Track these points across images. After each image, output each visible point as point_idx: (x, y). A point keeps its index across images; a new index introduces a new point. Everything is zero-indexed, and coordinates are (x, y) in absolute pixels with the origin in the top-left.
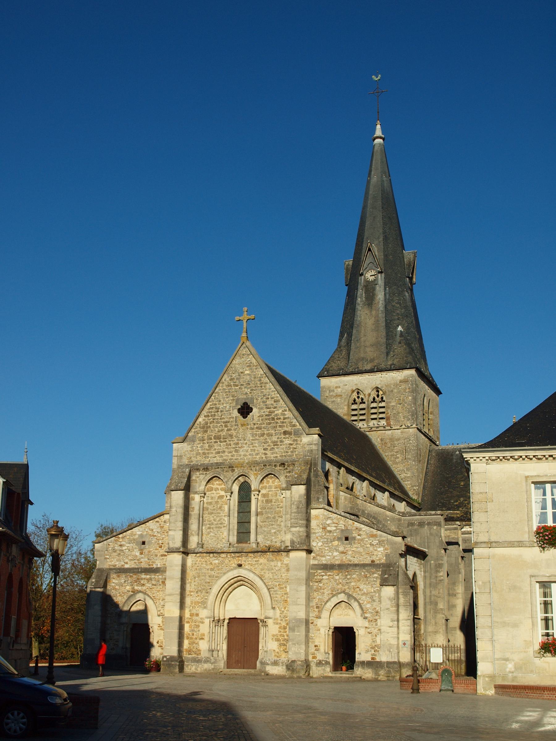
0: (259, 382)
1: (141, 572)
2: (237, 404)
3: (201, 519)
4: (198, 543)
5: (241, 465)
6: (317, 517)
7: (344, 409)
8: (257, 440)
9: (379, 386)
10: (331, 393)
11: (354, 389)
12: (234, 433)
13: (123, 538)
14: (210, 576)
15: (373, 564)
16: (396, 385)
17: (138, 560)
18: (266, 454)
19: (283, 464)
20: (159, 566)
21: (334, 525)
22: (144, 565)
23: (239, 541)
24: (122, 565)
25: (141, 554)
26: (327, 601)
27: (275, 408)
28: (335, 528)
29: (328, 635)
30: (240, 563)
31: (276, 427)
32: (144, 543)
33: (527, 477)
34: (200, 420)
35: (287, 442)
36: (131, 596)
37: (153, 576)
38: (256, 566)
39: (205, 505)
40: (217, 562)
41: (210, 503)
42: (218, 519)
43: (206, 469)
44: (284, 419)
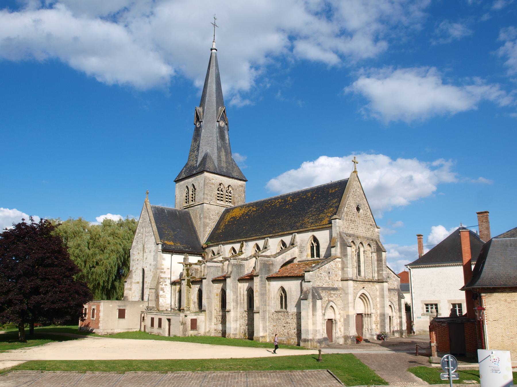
7: (215, 192)
9: (231, 185)
10: (210, 182)
13: (321, 269)
16: (238, 187)
17: (328, 283)
18: (366, 233)
19: (372, 240)
20: (336, 287)
22: (331, 286)
24: (322, 285)
25: (329, 279)
32: (329, 272)
37: (336, 292)
40: (356, 285)
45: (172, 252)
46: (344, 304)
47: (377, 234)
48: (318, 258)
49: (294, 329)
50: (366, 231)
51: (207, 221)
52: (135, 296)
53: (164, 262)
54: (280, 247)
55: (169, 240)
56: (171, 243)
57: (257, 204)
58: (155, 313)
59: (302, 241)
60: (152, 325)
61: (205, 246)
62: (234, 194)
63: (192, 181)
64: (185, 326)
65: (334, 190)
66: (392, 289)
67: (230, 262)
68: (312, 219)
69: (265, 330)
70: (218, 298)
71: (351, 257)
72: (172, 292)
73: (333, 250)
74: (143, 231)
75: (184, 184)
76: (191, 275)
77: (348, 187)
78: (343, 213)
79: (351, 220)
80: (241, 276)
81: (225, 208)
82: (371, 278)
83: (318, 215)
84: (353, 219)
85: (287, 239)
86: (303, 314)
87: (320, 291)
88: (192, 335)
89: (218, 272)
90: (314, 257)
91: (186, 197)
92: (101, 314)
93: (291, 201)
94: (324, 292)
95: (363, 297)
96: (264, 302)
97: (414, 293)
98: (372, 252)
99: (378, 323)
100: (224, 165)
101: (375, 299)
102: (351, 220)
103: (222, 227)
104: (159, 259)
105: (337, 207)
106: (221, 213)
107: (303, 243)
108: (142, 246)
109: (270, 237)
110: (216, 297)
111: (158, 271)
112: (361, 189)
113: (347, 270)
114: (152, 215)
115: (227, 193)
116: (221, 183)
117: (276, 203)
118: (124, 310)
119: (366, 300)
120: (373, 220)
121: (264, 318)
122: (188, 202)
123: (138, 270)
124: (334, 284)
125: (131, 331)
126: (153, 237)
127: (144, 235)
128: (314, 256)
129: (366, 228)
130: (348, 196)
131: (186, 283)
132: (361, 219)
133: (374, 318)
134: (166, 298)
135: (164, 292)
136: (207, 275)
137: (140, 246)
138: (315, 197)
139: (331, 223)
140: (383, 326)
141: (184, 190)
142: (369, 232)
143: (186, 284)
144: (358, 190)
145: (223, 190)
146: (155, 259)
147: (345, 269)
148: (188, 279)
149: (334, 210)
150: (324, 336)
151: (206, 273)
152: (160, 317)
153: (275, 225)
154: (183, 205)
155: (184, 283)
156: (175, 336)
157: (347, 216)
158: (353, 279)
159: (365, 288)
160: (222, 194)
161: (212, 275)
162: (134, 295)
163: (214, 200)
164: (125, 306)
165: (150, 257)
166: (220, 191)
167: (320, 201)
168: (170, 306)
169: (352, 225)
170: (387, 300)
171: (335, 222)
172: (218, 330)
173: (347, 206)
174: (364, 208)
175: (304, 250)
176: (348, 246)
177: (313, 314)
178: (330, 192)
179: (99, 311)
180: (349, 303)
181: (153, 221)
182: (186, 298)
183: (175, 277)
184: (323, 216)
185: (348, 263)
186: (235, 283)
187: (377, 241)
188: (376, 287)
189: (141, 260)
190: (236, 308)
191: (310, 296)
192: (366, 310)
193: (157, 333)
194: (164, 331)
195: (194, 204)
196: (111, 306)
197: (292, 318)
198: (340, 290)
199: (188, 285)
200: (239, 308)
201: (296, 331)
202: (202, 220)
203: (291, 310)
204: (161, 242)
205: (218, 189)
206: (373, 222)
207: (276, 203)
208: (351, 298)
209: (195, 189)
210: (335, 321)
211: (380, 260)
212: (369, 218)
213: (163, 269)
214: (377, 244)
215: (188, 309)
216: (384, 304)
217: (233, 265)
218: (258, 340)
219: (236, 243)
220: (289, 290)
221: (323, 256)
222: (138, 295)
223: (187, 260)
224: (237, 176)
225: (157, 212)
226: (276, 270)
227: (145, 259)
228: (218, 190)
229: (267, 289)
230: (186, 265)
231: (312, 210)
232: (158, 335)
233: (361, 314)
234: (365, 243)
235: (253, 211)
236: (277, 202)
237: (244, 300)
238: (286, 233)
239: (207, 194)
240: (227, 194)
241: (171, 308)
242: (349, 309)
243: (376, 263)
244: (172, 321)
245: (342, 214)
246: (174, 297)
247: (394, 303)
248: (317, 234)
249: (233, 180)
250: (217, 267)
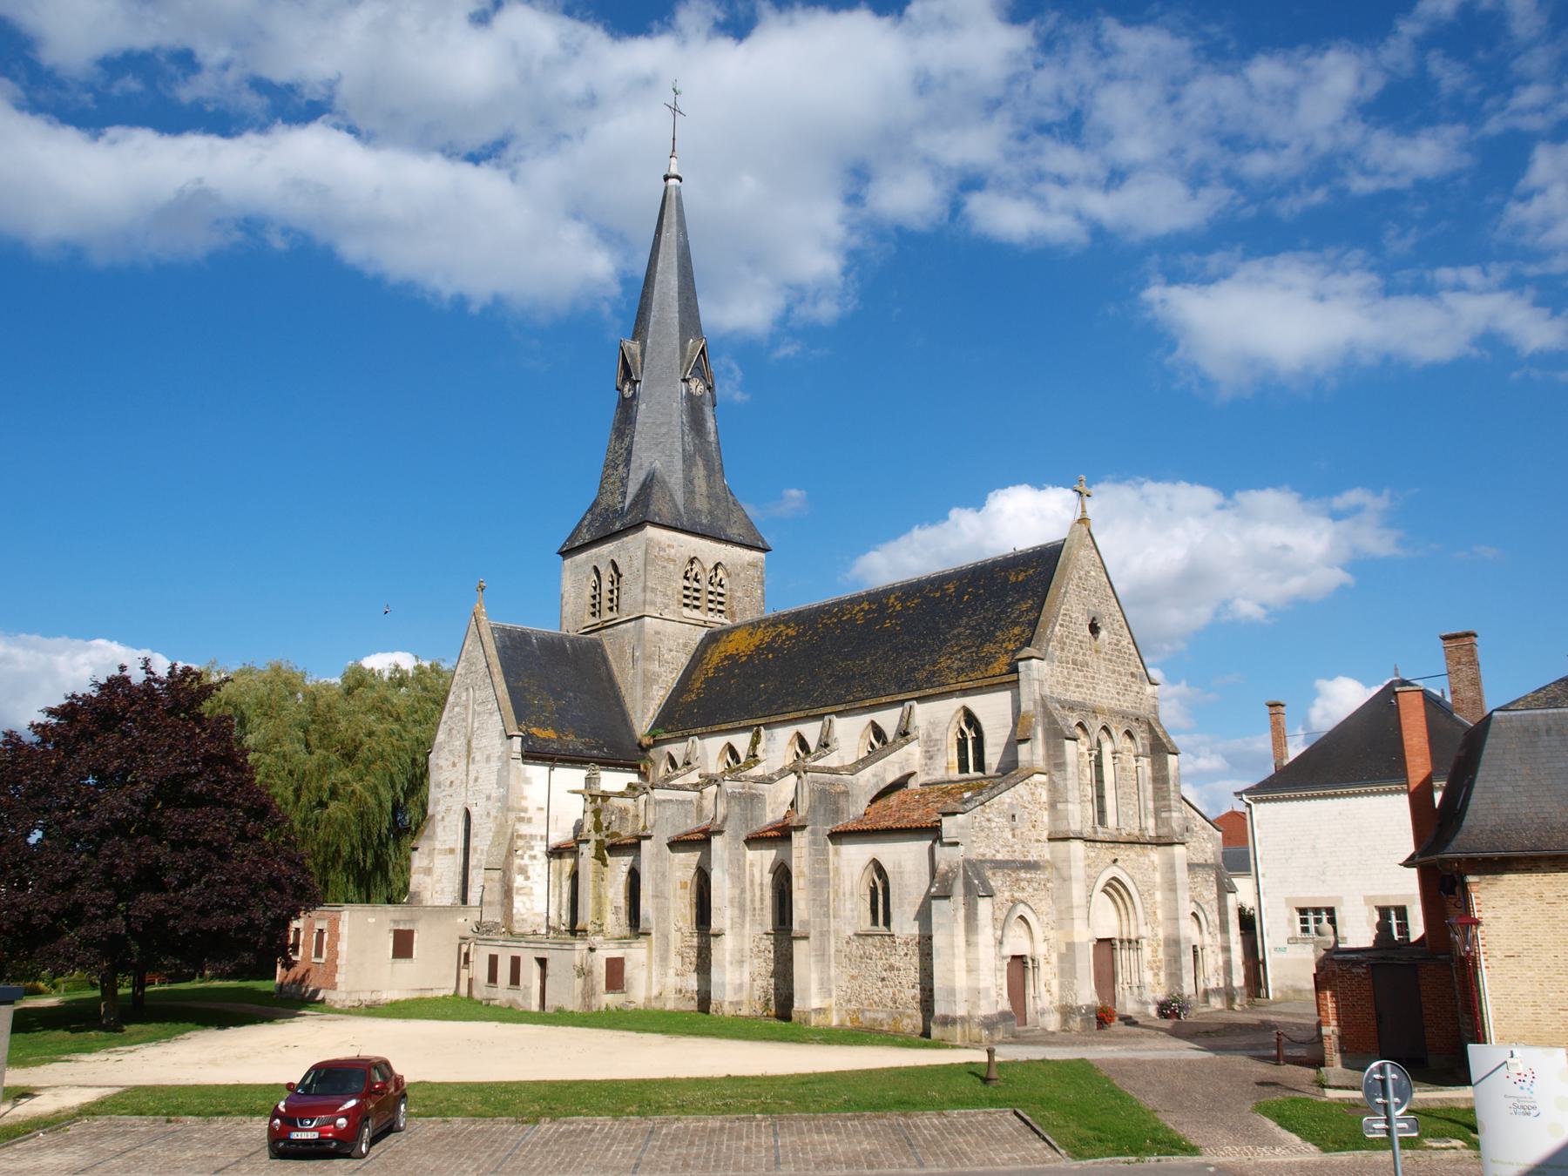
7: (677, 583)
9: (723, 563)
10: (662, 553)
15: (1204, 866)
16: (742, 566)
18: (1119, 700)
19: (1137, 719)
22: (1018, 856)
24: (994, 855)
25: (1014, 836)
31: (1123, 664)
32: (1013, 816)
36: (1012, 907)
40: (1093, 854)
45: (551, 759)
46: (1060, 912)
47: (1152, 701)
48: (979, 774)
49: (913, 987)
50: (1118, 693)
51: (655, 667)
52: (442, 889)
53: (528, 790)
54: (867, 742)
55: (542, 725)
56: (550, 734)
57: (798, 618)
58: (501, 943)
59: (933, 724)
60: (493, 977)
61: (646, 741)
62: (731, 590)
63: (611, 551)
64: (589, 979)
65: (1023, 574)
66: (1199, 865)
67: (723, 788)
68: (960, 660)
69: (825, 989)
70: (688, 896)
71: (1075, 770)
72: (551, 878)
73: (1023, 750)
74: (467, 700)
75: (586, 562)
76: (607, 828)
77: (1065, 566)
78: (1049, 640)
79: (1074, 662)
80: (755, 828)
81: (706, 629)
82: (1137, 832)
83: (978, 647)
84: (1080, 658)
85: (889, 719)
86: (938, 941)
87: (989, 873)
88: (610, 1004)
89: (686, 817)
90: (968, 772)
91: (594, 597)
92: (343, 946)
93: (898, 608)
94: (1001, 874)
95: (1115, 888)
96: (823, 907)
97: (1263, 875)
98: (1137, 756)
99: (1159, 968)
100: (702, 504)
101: (1150, 895)
102: (1074, 662)
103: (698, 685)
104: (512, 781)
105: (1034, 624)
106: (694, 645)
107: (934, 730)
108: (465, 742)
109: (839, 714)
110: (680, 892)
111: (512, 816)
112: (1103, 570)
113: (1067, 810)
114: (495, 652)
115: (712, 584)
116: (695, 558)
117: (856, 614)
118: (411, 933)
119: (1122, 899)
120: (1138, 660)
121: (823, 955)
122: (597, 614)
123: (452, 812)
124: (1028, 852)
125: (428, 995)
126: (497, 717)
127: (471, 711)
128: (968, 767)
129: (1118, 684)
130: (1063, 591)
131: (593, 853)
132: (1104, 659)
133: (1147, 953)
134: (532, 898)
135: (527, 878)
136: (653, 826)
137: (458, 743)
138: (969, 594)
139: (1015, 670)
140: (1175, 976)
141: (588, 580)
142: (1127, 697)
143: (593, 854)
144: (1093, 573)
145: (699, 577)
146: (502, 781)
147: (1060, 806)
148: (599, 838)
149: (1023, 632)
150: (1000, 1008)
151: (652, 821)
152: (516, 952)
153: (853, 677)
154: (583, 622)
155: (587, 851)
156: (560, 1010)
157: (1063, 649)
158: (1085, 835)
159: (1119, 863)
160: (696, 590)
161: (669, 826)
162: (438, 889)
163: (674, 606)
164: (412, 921)
165: (487, 774)
166: (691, 580)
167: (982, 608)
168: (544, 919)
169: (1078, 676)
170: (1184, 897)
171: (1028, 668)
172: (687, 992)
173: (1063, 620)
174: (1112, 624)
175: (939, 750)
176: (1067, 739)
177: (967, 941)
178: (1012, 578)
179: (335, 936)
180: (1072, 907)
181: (497, 668)
182: (591, 896)
183: (559, 834)
184: (993, 651)
185: (1069, 787)
186: (736, 849)
187: (1152, 721)
188: (1152, 858)
189: (462, 783)
190: (739, 923)
191: (959, 888)
192: (1125, 929)
193: (508, 1001)
194: (527, 996)
195: (615, 619)
196: (372, 920)
197: (906, 955)
198: (1045, 868)
199: (600, 857)
200: (747, 925)
201: (917, 991)
202: (640, 665)
203: (901, 929)
204: (520, 730)
205: (686, 573)
206: (1138, 667)
207: (856, 614)
208: (1078, 891)
209: (620, 576)
210: (1033, 960)
211: (1160, 778)
212: (1126, 656)
213: (525, 810)
214: (1151, 730)
215: (597, 928)
216: (1177, 909)
217: (732, 797)
218: (807, 1021)
219: (736, 733)
220: (897, 870)
221: (995, 767)
222: (451, 889)
223: (595, 784)
224: (740, 535)
225: (508, 643)
226: (857, 809)
227: (471, 782)
228: (686, 578)
229: (831, 867)
230: (594, 797)
231: (959, 634)
232: (510, 1007)
233: (1110, 940)
234: (1116, 728)
235: (789, 638)
236: (858, 612)
237: (762, 900)
238: (884, 700)
239: (653, 590)
240: (711, 588)
241: (548, 927)
242: (1072, 926)
243: (1150, 787)
244: (550, 964)
245: (1048, 645)
246: (557, 892)
247: (1205, 907)
248: (977, 703)
249: (729, 547)
250: (682, 802)
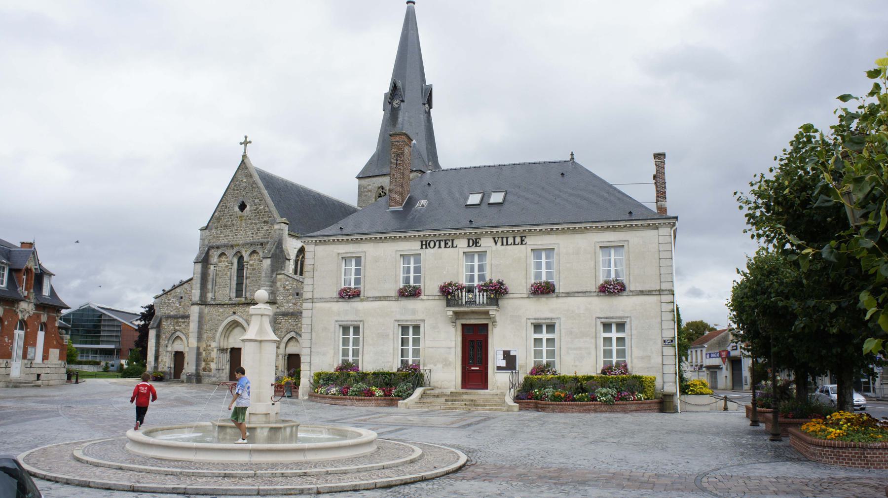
0: (251, 188)
1: (179, 318)
2: (238, 202)
3: (214, 281)
4: (212, 298)
5: (239, 245)
6: (280, 279)
8: (248, 227)
11: (379, 186)
12: (234, 222)
14: (217, 320)
18: (253, 237)
21: (290, 285)
23: (237, 297)
24: (170, 313)
25: (180, 305)
26: (284, 337)
27: (260, 205)
28: (290, 287)
29: (285, 359)
30: (235, 311)
32: (182, 298)
33: (339, 254)
34: (216, 214)
35: (266, 228)
36: (174, 333)
38: (244, 313)
39: (217, 272)
40: (222, 310)
41: (220, 271)
42: (224, 281)
43: (218, 248)
44: (265, 212)
144: (245, 180)
169: (227, 232)
